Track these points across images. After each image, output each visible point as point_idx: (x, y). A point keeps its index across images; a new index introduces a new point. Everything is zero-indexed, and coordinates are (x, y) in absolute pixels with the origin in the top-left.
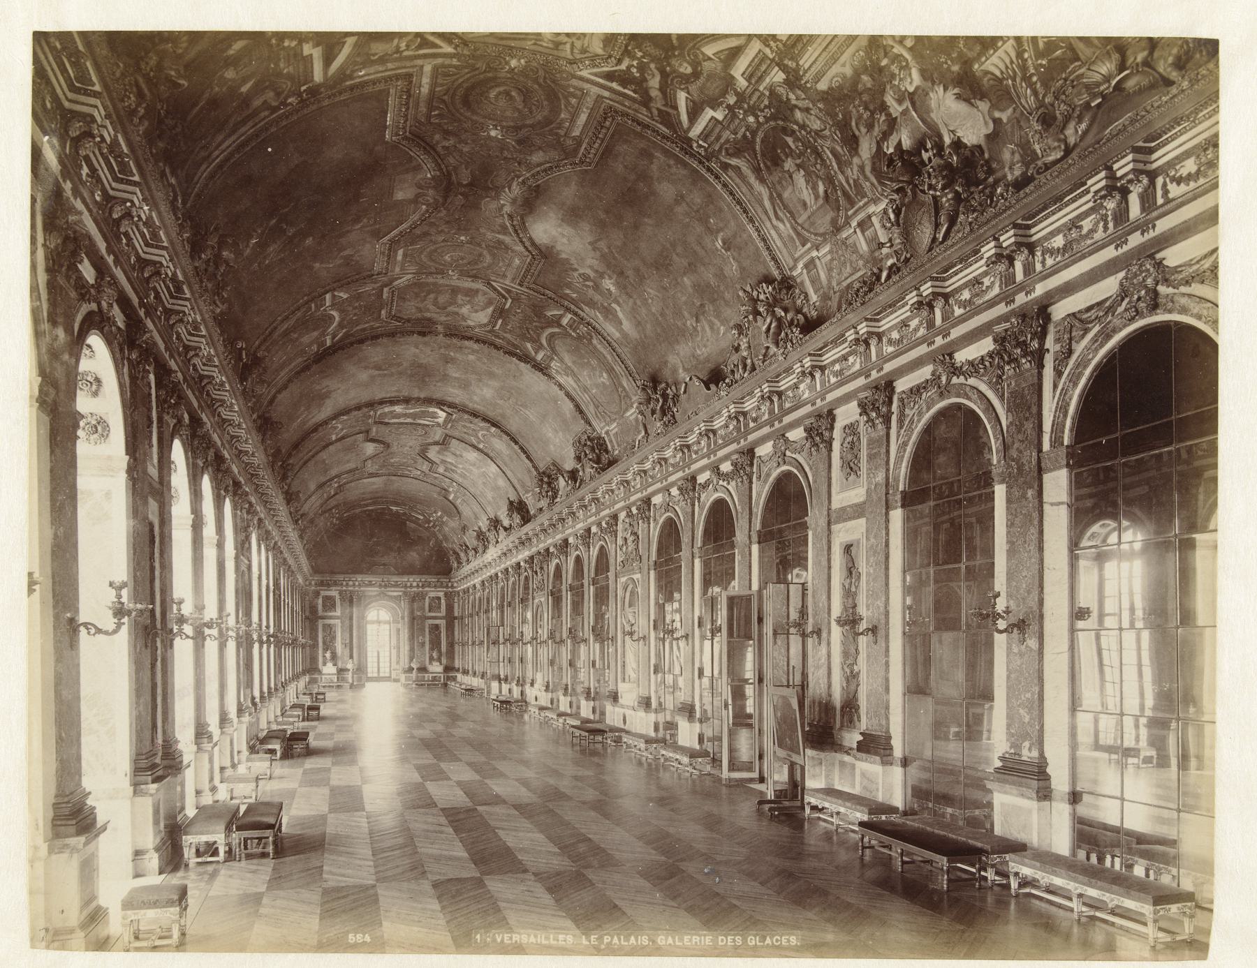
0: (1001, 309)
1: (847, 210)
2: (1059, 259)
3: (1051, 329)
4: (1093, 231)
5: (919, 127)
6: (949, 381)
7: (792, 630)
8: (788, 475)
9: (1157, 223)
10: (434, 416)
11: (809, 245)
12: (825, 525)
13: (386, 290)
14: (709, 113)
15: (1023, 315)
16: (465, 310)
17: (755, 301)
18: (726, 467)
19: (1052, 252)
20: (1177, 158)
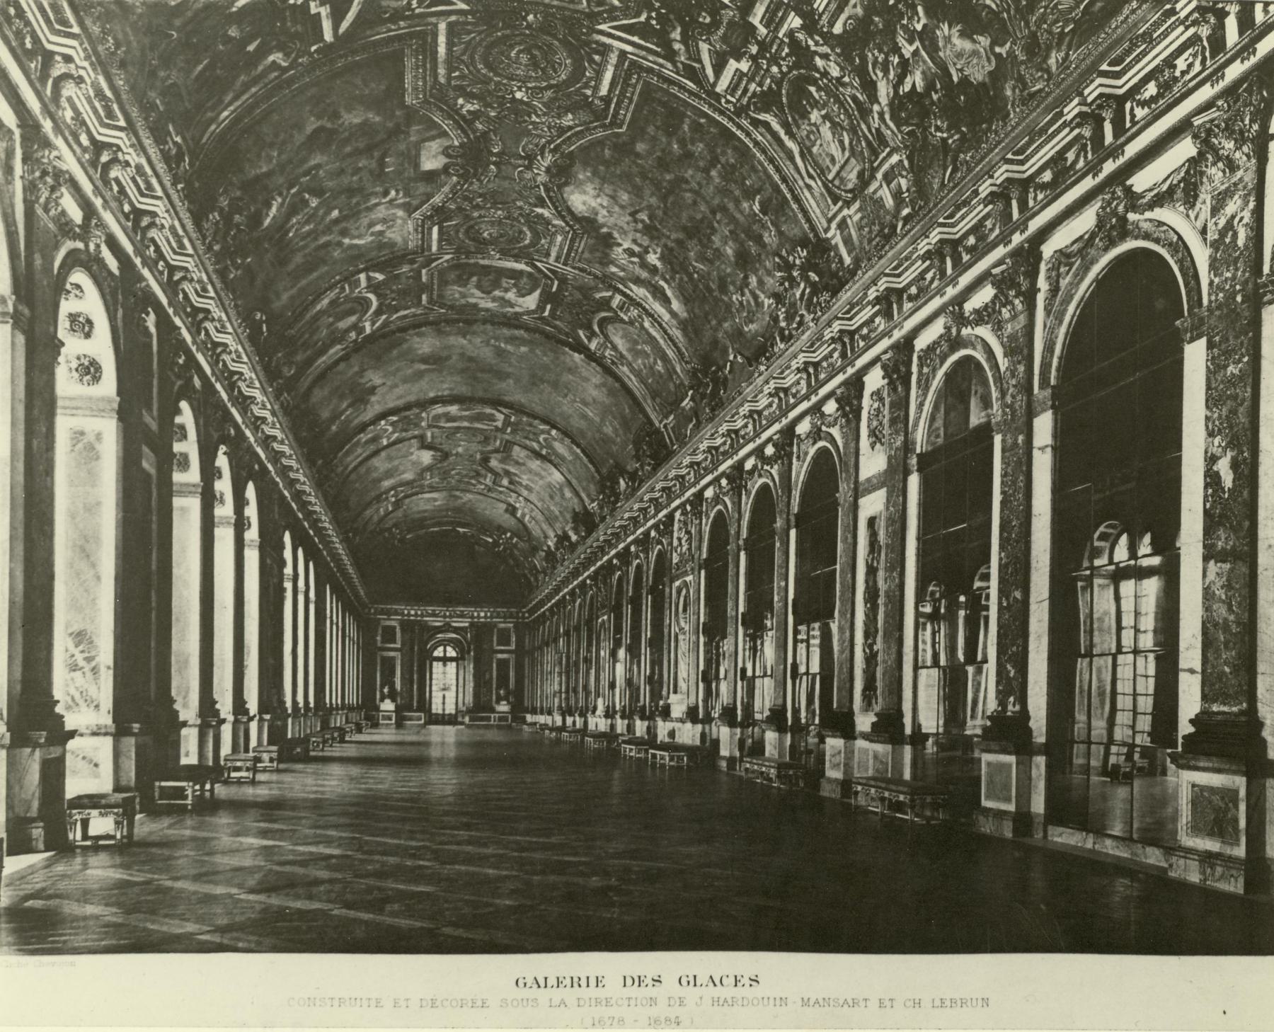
1: (872, 162)
5: (930, 69)
10: (491, 418)
11: (840, 204)
13: (424, 271)
14: (732, 65)
16: (511, 296)
17: (788, 267)
18: (770, 450)
19: (1044, 187)
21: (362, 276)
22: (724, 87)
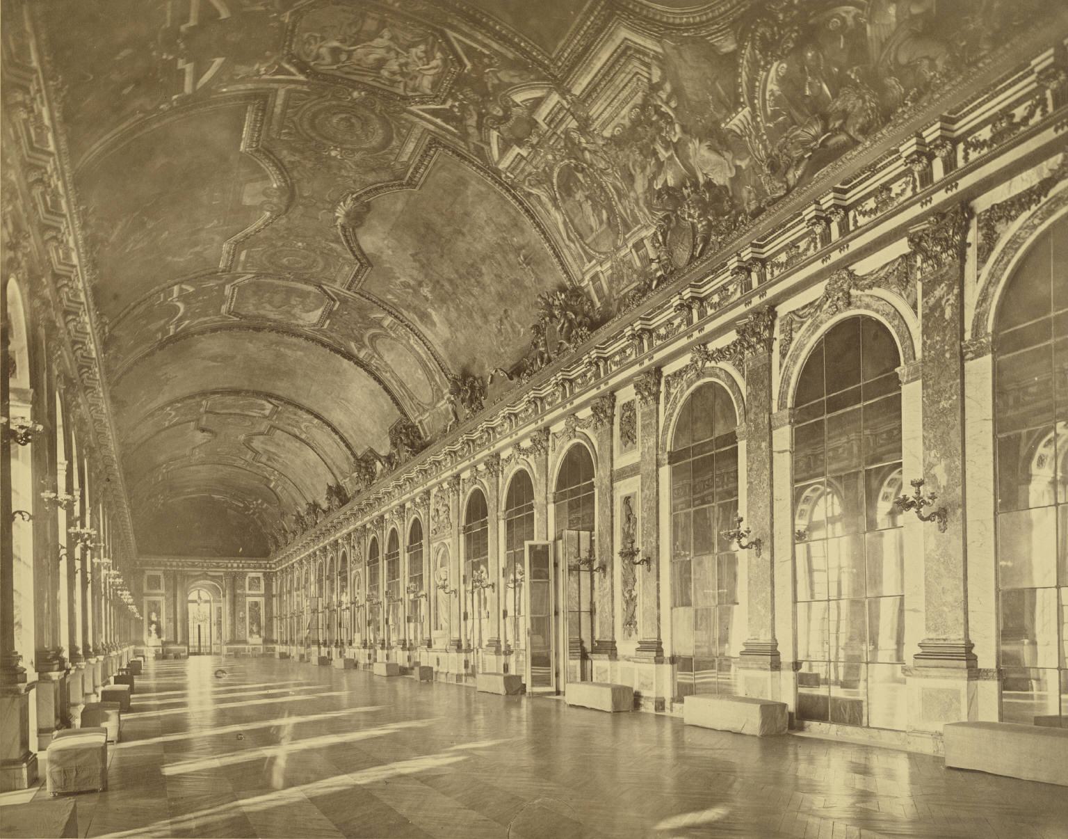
0: (742, 309)
1: (625, 234)
2: (783, 270)
3: (777, 323)
4: (807, 249)
6: (703, 364)
7: (582, 567)
8: (578, 446)
11: (594, 262)
12: (608, 484)
15: (757, 312)
18: (526, 444)
19: (779, 265)
20: (862, 197)
21: (176, 288)
22: (506, 166)
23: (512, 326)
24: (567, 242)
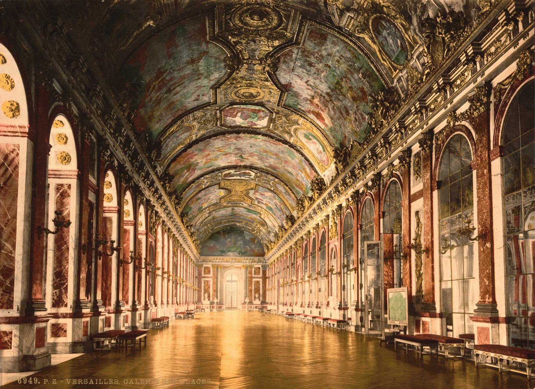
1: (411, 51)
4: (505, 41)
9: (530, 33)
11: (398, 71)
17: (376, 100)
18: (370, 184)
19: (490, 54)
22: (344, 23)
23: (362, 115)
24: (382, 62)
